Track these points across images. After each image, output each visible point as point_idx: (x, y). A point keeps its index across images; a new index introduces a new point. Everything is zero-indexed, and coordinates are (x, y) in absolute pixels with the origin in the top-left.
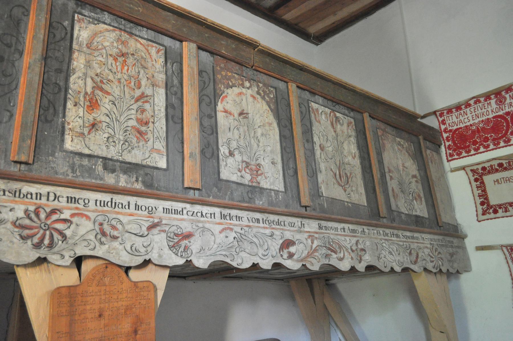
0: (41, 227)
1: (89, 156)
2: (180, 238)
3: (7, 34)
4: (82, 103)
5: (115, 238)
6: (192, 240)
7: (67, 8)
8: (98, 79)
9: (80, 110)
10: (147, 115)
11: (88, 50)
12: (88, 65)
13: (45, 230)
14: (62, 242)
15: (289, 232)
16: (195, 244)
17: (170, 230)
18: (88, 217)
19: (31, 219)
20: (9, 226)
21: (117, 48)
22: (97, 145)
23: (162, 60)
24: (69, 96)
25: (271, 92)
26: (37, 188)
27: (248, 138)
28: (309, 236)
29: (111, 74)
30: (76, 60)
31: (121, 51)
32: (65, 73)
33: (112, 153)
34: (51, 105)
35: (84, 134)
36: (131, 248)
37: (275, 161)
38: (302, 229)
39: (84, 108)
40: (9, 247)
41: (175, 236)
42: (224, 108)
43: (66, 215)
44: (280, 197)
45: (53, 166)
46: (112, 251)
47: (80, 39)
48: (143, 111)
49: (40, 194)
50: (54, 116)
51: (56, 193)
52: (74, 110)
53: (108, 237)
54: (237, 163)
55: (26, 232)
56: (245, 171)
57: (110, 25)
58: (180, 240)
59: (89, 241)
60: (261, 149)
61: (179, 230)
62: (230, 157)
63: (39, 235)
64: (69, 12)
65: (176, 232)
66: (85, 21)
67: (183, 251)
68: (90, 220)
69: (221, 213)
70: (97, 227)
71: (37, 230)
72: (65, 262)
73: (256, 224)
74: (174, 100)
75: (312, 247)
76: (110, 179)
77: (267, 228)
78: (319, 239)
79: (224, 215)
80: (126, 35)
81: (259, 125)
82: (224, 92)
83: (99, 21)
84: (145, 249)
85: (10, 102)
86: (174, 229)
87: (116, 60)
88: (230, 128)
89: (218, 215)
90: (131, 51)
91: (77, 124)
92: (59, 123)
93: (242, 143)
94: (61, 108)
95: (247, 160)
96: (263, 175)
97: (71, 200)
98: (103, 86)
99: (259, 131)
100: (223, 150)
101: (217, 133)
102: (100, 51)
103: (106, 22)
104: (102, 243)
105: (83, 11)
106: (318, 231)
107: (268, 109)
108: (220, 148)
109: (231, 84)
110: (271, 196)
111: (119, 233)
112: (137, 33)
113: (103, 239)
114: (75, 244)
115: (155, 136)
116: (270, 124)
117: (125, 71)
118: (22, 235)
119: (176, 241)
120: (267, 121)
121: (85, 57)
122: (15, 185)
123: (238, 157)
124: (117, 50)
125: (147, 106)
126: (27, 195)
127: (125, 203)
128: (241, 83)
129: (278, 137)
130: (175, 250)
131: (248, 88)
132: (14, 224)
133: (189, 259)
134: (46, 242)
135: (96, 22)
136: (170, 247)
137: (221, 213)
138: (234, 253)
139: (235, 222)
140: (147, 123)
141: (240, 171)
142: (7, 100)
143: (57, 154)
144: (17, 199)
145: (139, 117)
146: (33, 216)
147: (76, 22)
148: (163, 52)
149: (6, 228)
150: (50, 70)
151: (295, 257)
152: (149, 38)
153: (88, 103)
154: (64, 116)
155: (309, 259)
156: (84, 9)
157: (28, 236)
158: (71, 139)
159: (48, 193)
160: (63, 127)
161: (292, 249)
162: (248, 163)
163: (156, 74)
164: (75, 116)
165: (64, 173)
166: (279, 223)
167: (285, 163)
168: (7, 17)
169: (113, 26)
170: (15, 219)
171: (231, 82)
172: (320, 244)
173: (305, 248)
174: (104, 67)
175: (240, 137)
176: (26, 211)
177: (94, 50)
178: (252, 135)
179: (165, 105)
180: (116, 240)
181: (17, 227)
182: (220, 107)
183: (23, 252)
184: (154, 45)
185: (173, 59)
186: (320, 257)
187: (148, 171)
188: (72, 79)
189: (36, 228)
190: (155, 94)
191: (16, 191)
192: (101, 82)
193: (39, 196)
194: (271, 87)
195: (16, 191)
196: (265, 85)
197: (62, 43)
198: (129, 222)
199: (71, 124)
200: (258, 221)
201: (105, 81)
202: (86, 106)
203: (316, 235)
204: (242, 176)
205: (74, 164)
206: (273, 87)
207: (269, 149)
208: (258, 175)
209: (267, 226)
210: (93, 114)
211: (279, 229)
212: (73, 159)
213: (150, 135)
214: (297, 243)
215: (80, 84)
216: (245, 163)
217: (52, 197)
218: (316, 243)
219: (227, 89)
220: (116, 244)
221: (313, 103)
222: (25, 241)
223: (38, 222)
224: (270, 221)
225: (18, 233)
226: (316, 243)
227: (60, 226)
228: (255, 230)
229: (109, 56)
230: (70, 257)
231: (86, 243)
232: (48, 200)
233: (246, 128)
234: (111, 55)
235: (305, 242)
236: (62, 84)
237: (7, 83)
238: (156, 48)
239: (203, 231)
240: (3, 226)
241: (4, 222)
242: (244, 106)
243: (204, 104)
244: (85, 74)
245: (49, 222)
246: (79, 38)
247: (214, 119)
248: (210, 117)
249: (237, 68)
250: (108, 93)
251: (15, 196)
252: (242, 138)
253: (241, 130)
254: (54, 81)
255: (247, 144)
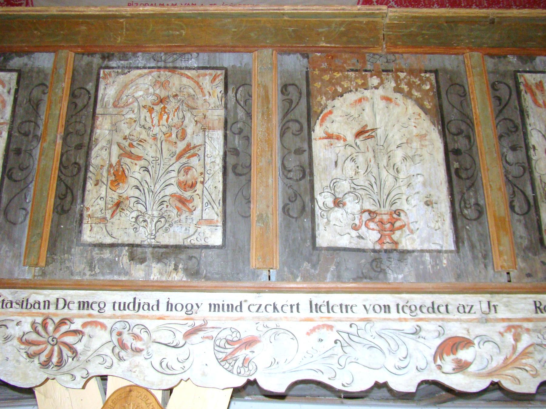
0: (49, 342)
1: (112, 246)
2: (236, 346)
3: (26, 122)
4: (104, 180)
5: (138, 351)
6: (256, 348)
7: (92, 66)
8: (126, 143)
9: (102, 189)
10: (194, 174)
11: (115, 109)
12: (115, 128)
13: (53, 345)
14: (73, 360)
15: (457, 324)
16: (261, 355)
17: (220, 336)
18: (103, 326)
19: (38, 333)
20: (16, 342)
21: (154, 94)
22: (123, 229)
23: (221, 88)
24: (89, 174)
25: (423, 82)
26: (45, 295)
27: (375, 171)
28: (509, 328)
29: (144, 131)
30: (99, 127)
31: (158, 96)
32: (86, 148)
33: (143, 236)
34: (69, 191)
35: (105, 218)
36: (161, 364)
37: (434, 199)
38: (492, 315)
39: (107, 186)
40: (15, 367)
41: (228, 344)
42: (326, 133)
43: (77, 325)
44: (445, 261)
45: (68, 265)
46: (134, 370)
47: (106, 99)
48: (187, 169)
49: (49, 302)
50: (71, 204)
51: (66, 298)
52: (95, 191)
53: (129, 351)
54: (351, 216)
55: (33, 349)
56: (366, 225)
57: (144, 68)
58: (236, 350)
59: (104, 356)
60: (402, 184)
61: (234, 335)
62: (336, 209)
63: (46, 352)
64: (94, 71)
65: (230, 338)
66: (113, 74)
67: (241, 365)
68: (106, 329)
69: (311, 302)
70: (115, 338)
71: (44, 346)
72: (76, 385)
73: (383, 315)
74: (237, 142)
75: (514, 348)
76: (138, 272)
77: (406, 320)
78: (534, 331)
79: (316, 305)
80: (167, 73)
81: (398, 143)
82: (326, 106)
83: (130, 68)
84: (181, 365)
85: (26, 198)
86: (226, 334)
87: (151, 110)
88: (336, 163)
89: (305, 307)
90: (174, 91)
91: (98, 207)
92: (77, 210)
93: (361, 180)
94: (80, 192)
95: (373, 208)
96: (405, 229)
97: (84, 305)
98: (133, 150)
99: (399, 154)
100: (323, 199)
101: (312, 174)
102: (131, 106)
103: (139, 65)
104: (120, 359)
105: (111, 63)
106: (535, 316)
107: (418, 110)
108: (317, 197)
109: (340, 90)
110: (423, 263)
111: (144, 344)
112: (184, 65)
113: (123, 354)
114: (88, 361)
115: (205, 201)
116: (422, 137)
117: (164, 122)
118: (29, 352)
119: (229, 351)
120: (415, 131)
121: (112, 118)
122: (22, 294)
123: (352, 206)
124: (154, 97)
125: (194, 161)
126: (34, 304)
127: (153, 302)
128: (360, 82)
129: (440, 156)
130: (227, 366)
131: (376, 88)
132: (20, 340)
133: (252, 379)
134: (55, 359)
135: (126, 71)
136: (220, 361)
137: (311, 302)
138: (336, 366)
139: (337, 314)
140: (193, 186)
141: (355, 228)
142: (23, 196)
143: (73, 250)
144: (24, 310)
145: (182, 178)
146: (40, 329)
147: (101, 79)
148: (222, 77)
149: (12, 345)
150: (70, 149)
151: (472, 369)
152: (201, 65)
153: (113, 178)
154: (83, 201)
155: (509, 372)
156: (112, 60)
157: (34, 353)
158: (89, 228)
159: (58, 300)
160: (81, 215)
161: (464, 354)
162: (374, 212)
163: (209, 113)
164: (96, 197)
165: (80, 272)
166: (434, 308)
167: (457, 198)
168: (27, 102)
169: (149, 68)
170: (22, 334)
171: (342, 86)
172: (539, 341)
173: (496, 350)
174: (134, 124)
175: (357, 173)
176: (33, 324)
177: (123, 107)
178: (384, 162)
179: (222, 153)
180: (138, 354)
181: (23, 343)
182: (318, 131)
183: (30, 372)
184: (208, 72)
185: (234, 82)
186: (537, 366)
187: (191, 252)
188: (93, 153)
189: (43, 343)
190: (207, 140)
191: (23, 301)
192: (131, 145)
193: (47, 304)
194: (426, 72)
195: (23, 301)
196: (411, 72)
197: (84, 112)
198: (158, 329)
199: (91, 209)
200: (387, 309)
201: (135, 143)
202: (109, 182)
203: (529, 325)
204: (360, 237)
205: (92, 258)
206: (431, 71)
207: (420, 179)
208: (393, 230)
209: (408, 316)
210: (118, 191)
211: (433, 319)
212: (91, 253)
213: (197, 202)
214: (476, 341)
215: (103, 156)
216: (367, 213)
217: (61, 304)
218: (526, 340)
219: (333, 99)
220: (139, 359)
221: (527, 75)
222: (32, 360)
223: (46, 336)
224: (413, 308)
225: (24, 351)
226: (526, 340)
227: (69, 339)
228: (378, 326)
229: (142, 109)
230: (82, 377)
231: (100, 360)
232: (57, 308)
233: (370, 155)
234: (144, 107)
235: (497, 339)
236: (82, 162)
237: (24, 177)
238: (211, 74)
239: (276, 334)
240: (9, 343)
241: (10, 339)
242: (367, 118)
243: (289, 135)
244: (110, 142)
245: (57, 335)
246: (104, 99)
247: (306, 154)
248: (299, 152)
249: (354, 61)
250: (139, 158)
251: (22, 307)
252: (362, 171)
253: (361, 159)
254: (73, 161)
255: (373, 180)
